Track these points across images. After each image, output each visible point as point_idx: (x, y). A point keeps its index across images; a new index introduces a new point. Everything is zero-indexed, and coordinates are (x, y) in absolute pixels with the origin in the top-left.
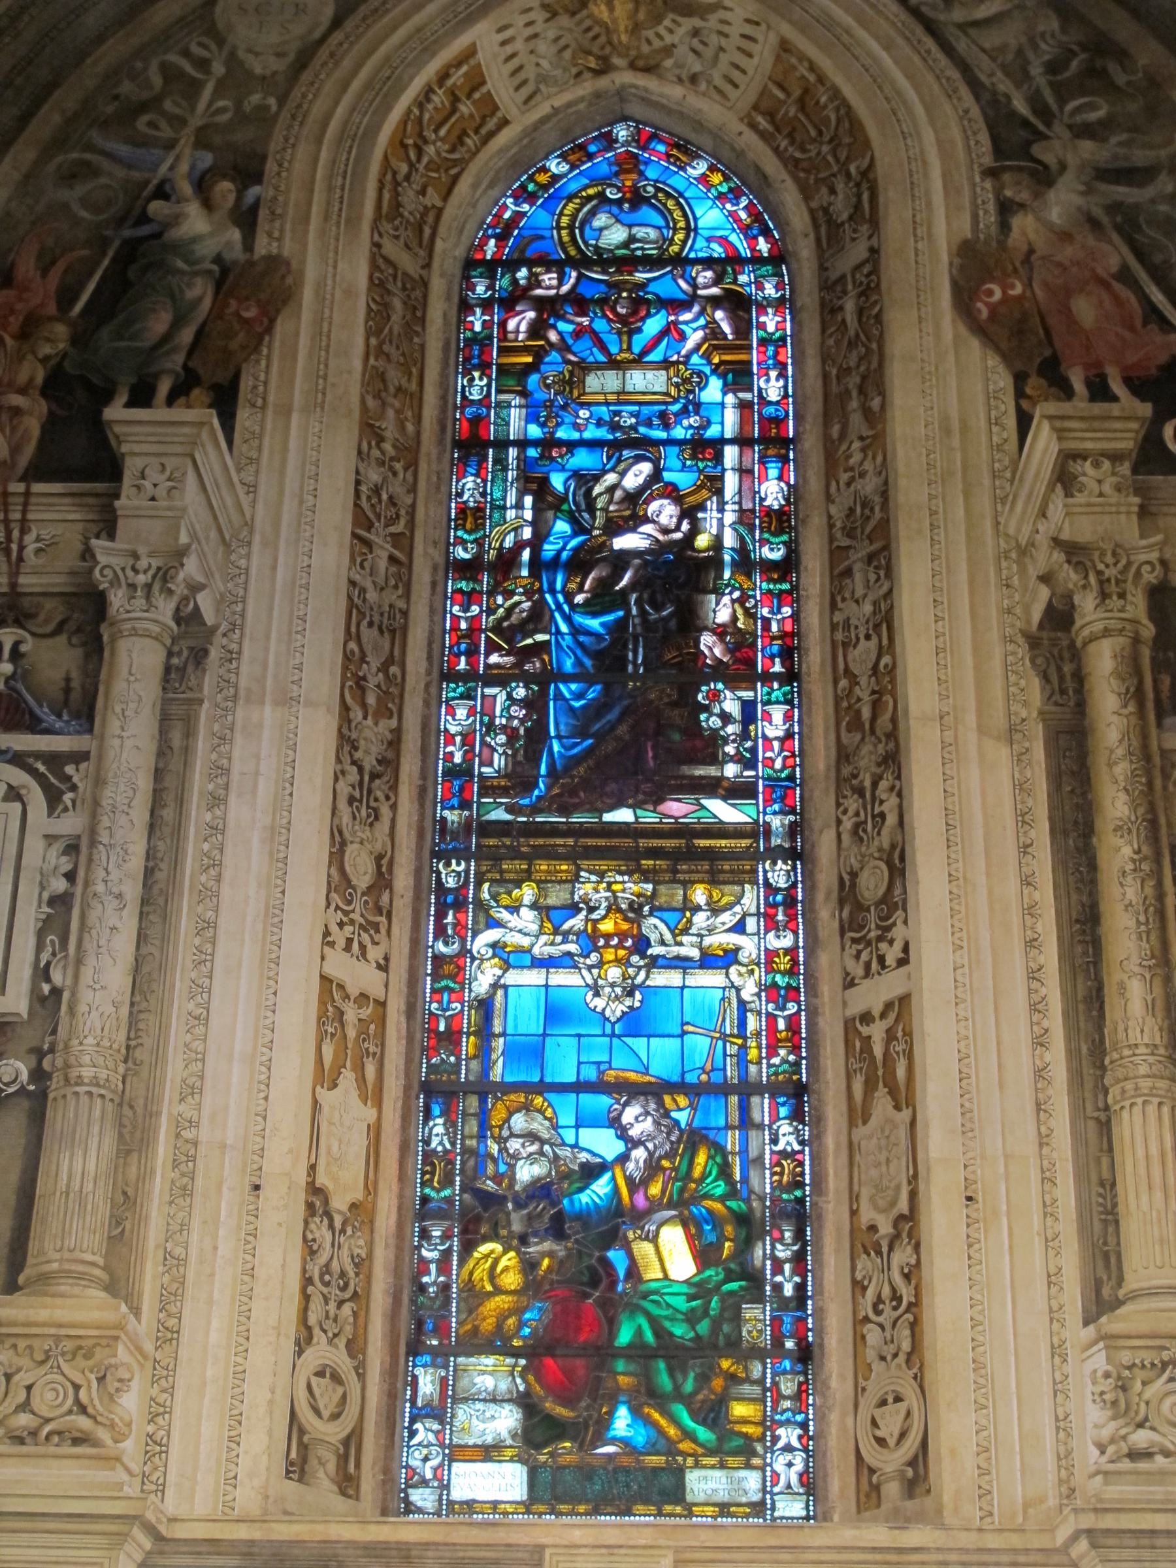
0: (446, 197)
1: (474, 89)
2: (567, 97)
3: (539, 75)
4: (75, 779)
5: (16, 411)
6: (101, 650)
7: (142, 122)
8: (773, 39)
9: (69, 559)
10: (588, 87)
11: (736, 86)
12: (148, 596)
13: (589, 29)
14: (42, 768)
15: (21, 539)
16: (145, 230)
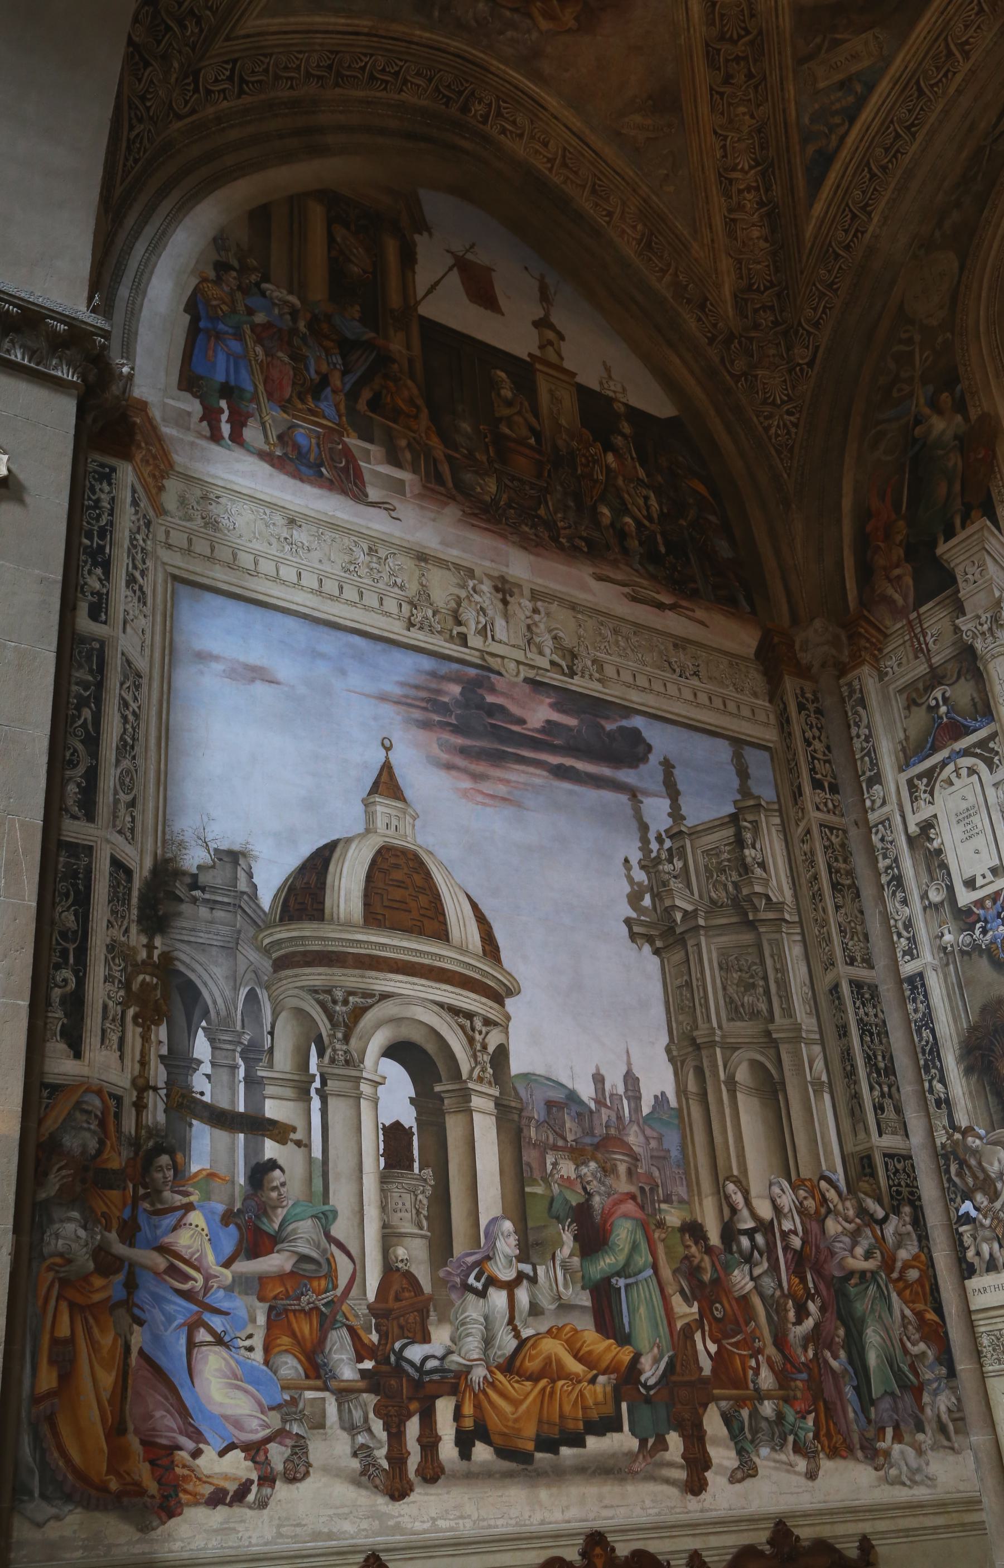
4: (996, 749)
5: (899, 577)
6: (981, 675)
7: (895, 394)
9: (949, 638)
12: (992, 635)
14: (979, 751)
15: (925, 640)
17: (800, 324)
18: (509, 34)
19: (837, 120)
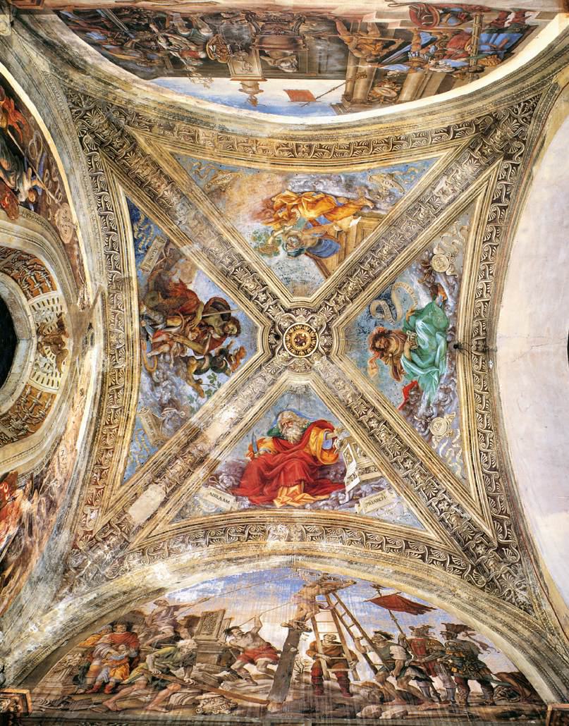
0: (13, 278)
1: (42, 289)
2: (31, 320)
3: (40, 311)
8: (55, 392)
10: (34, 328)
11: (37, 380)
13: (51, 328)
16: (26, 166)
17: (97, 151)
18: (302, 183)
19: (140, 236)
